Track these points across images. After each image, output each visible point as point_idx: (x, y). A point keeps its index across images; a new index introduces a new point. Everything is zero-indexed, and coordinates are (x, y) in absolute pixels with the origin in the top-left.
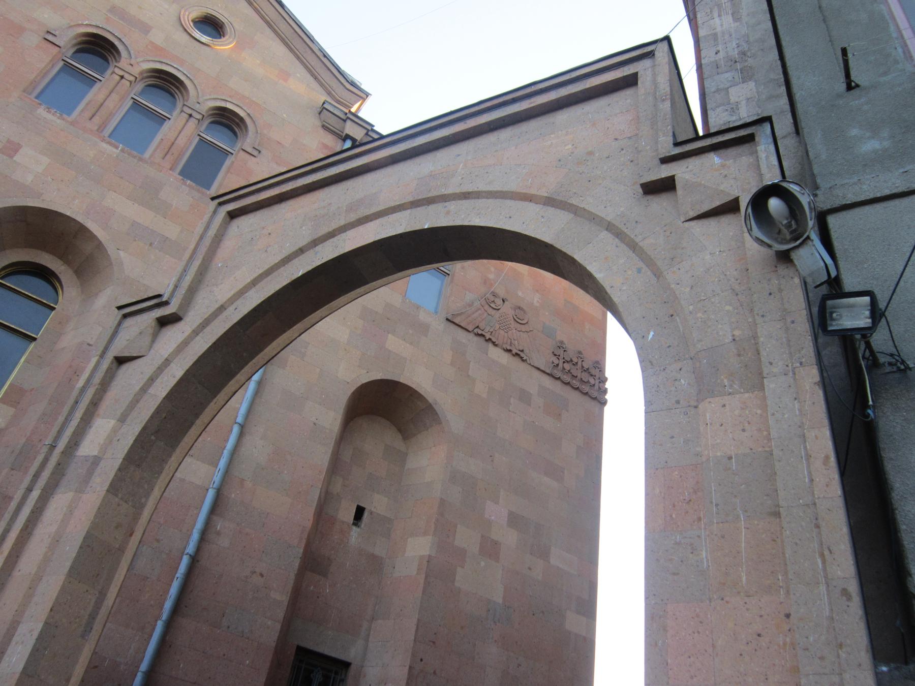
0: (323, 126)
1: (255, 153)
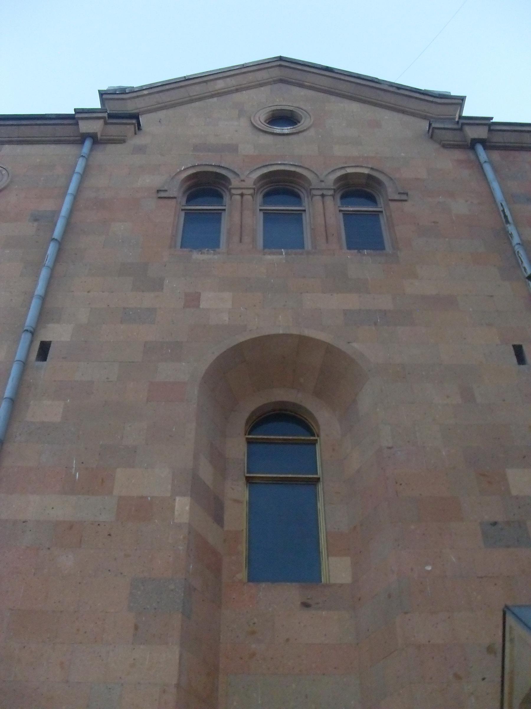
0: (444, 146)
1: (404, 197)
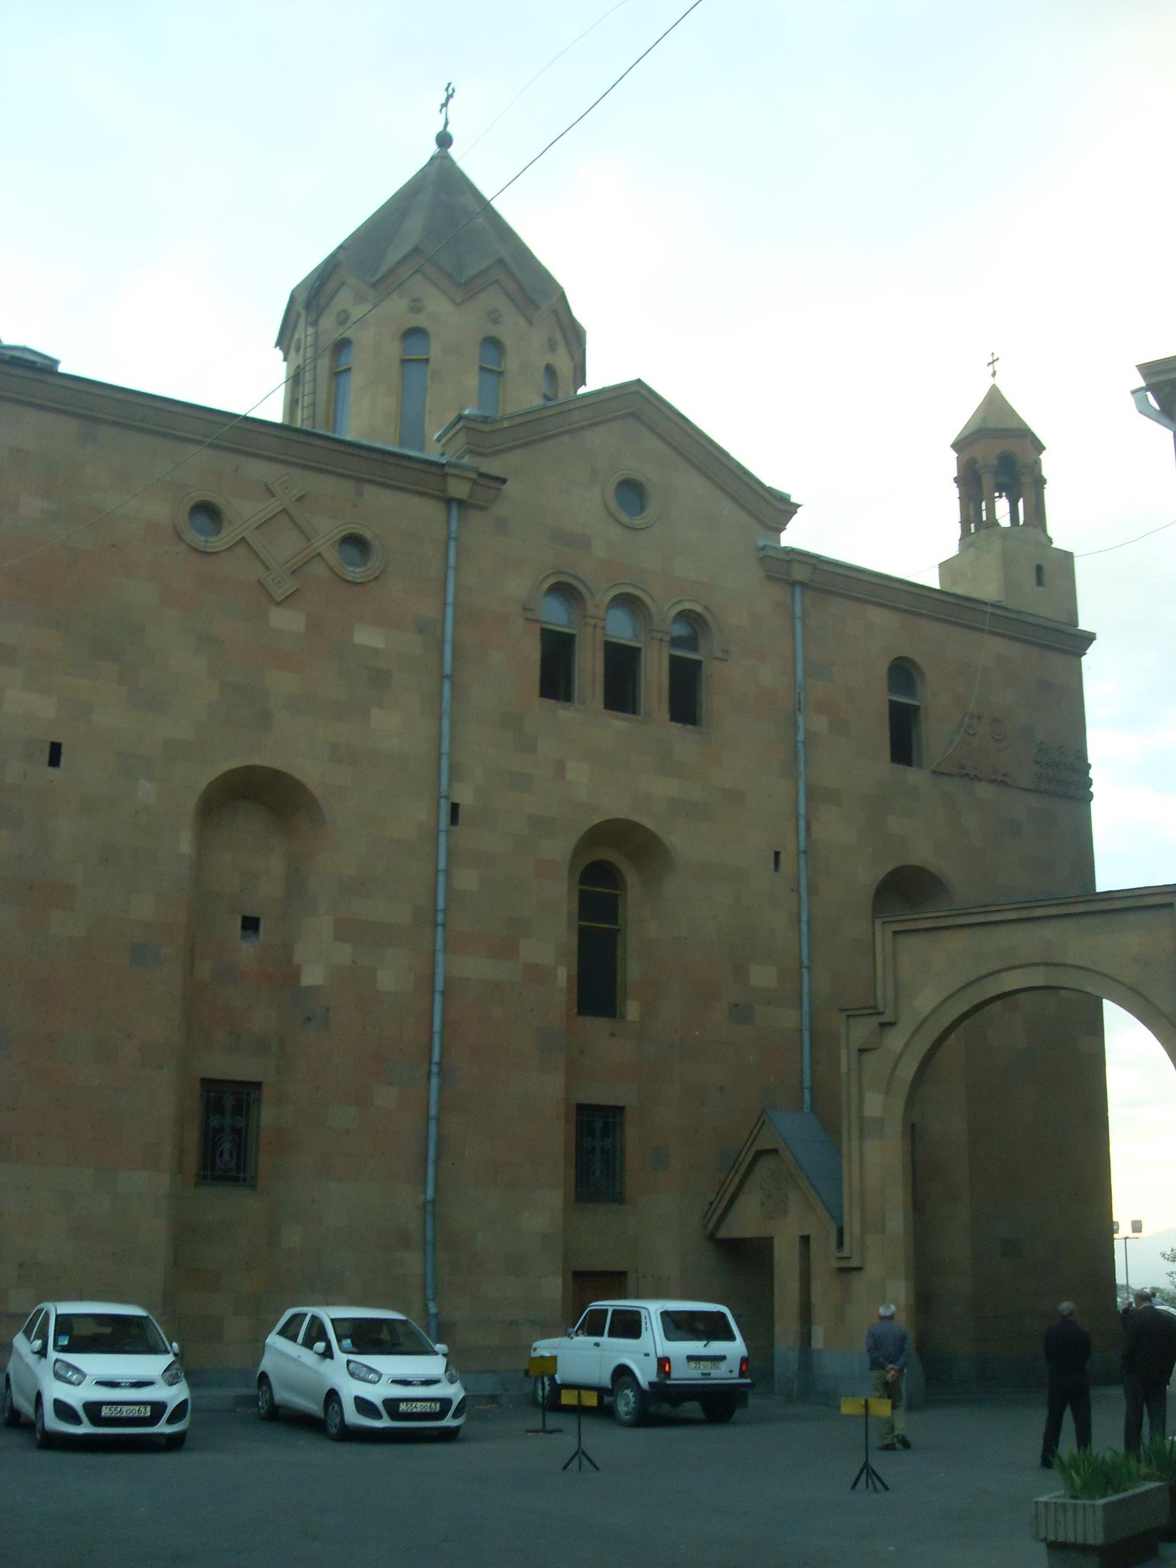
0: (770, 578)
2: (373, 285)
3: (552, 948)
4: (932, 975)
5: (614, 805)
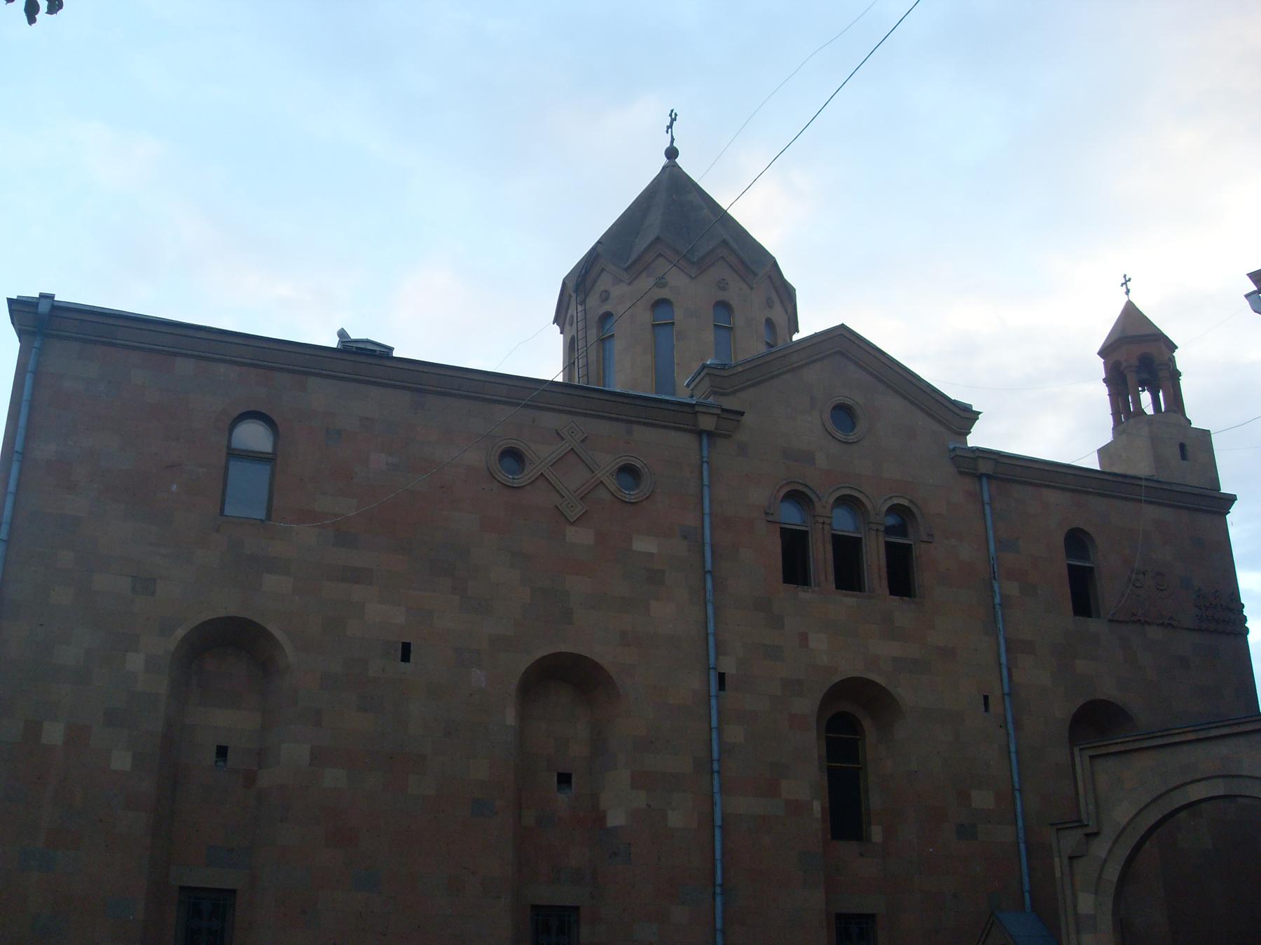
0: (961, 473)
2: (626, 269)
3: (806, 785)
4: (1126, 792)
5: (850, 667)
